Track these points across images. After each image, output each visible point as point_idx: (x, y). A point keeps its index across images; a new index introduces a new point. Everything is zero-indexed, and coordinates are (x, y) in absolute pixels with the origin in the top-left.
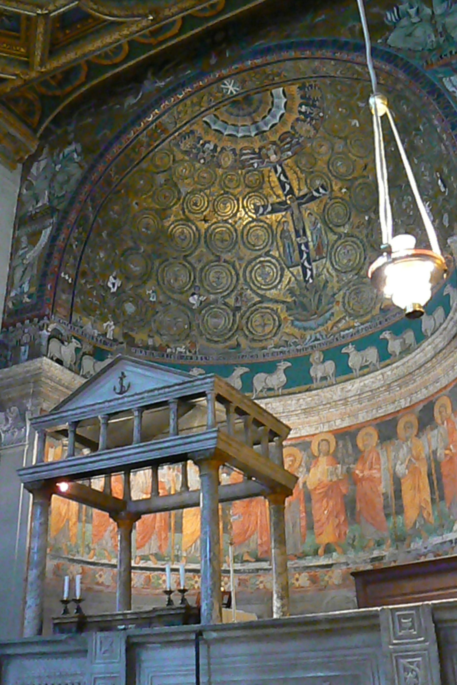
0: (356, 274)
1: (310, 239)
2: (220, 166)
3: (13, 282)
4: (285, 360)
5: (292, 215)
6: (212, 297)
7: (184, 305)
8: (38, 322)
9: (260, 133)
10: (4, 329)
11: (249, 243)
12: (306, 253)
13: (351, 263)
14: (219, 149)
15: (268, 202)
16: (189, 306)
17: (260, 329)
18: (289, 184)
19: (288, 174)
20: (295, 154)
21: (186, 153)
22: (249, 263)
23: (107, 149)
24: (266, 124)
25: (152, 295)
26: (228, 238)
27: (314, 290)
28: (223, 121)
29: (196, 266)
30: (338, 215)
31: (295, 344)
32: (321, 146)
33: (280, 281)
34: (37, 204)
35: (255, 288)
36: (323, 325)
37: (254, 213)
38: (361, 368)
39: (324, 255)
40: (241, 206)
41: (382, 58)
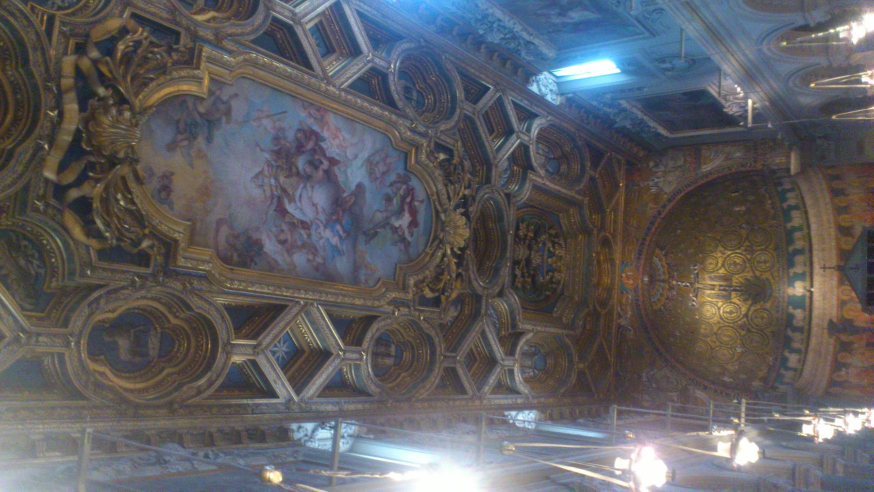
6: (739, 341)
9: (664, 281)
16: (742, 353)
17: (765, 320)
38: (805, 265)
41: (676, 196)
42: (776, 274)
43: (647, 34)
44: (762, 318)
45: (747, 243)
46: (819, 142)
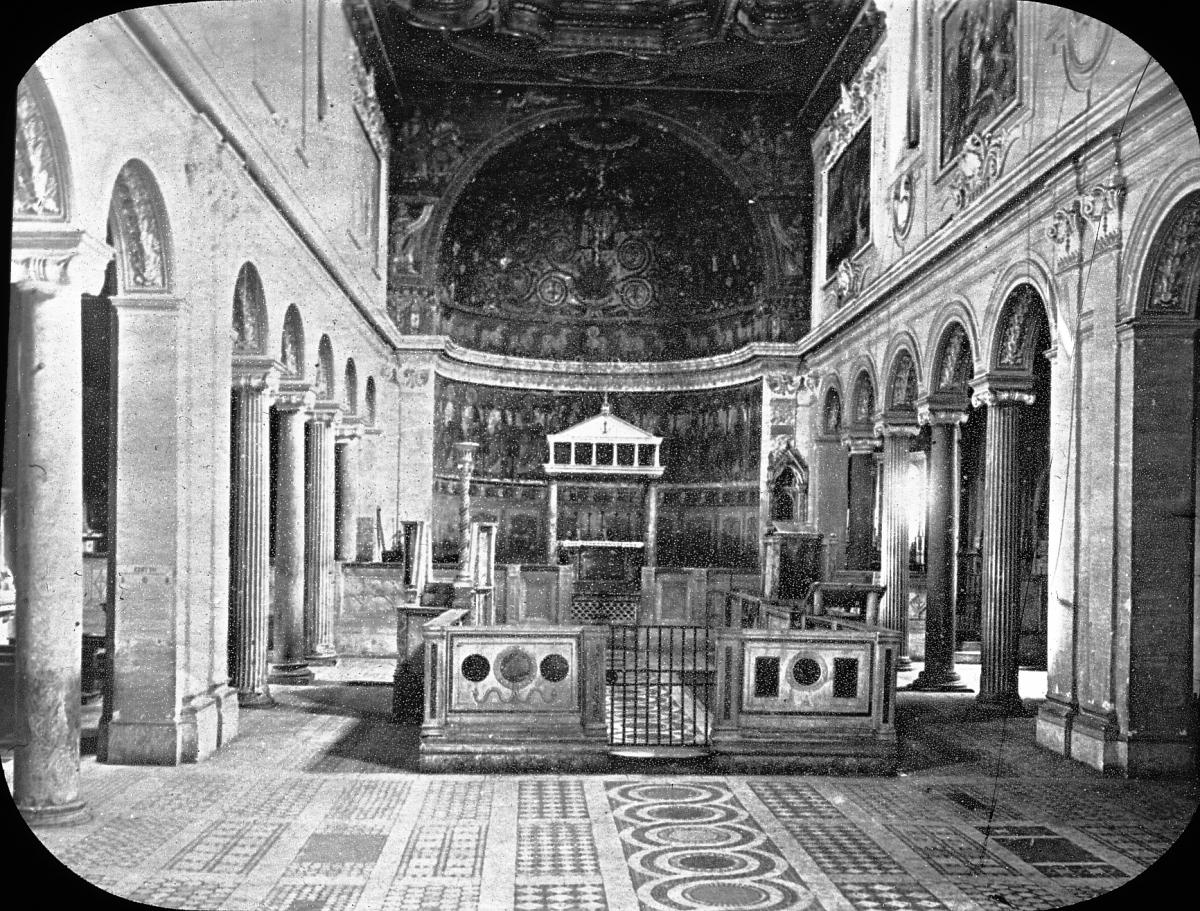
17: (550, 296)
43: (940, 173)
44: (554, 293)
46: (797, 379)
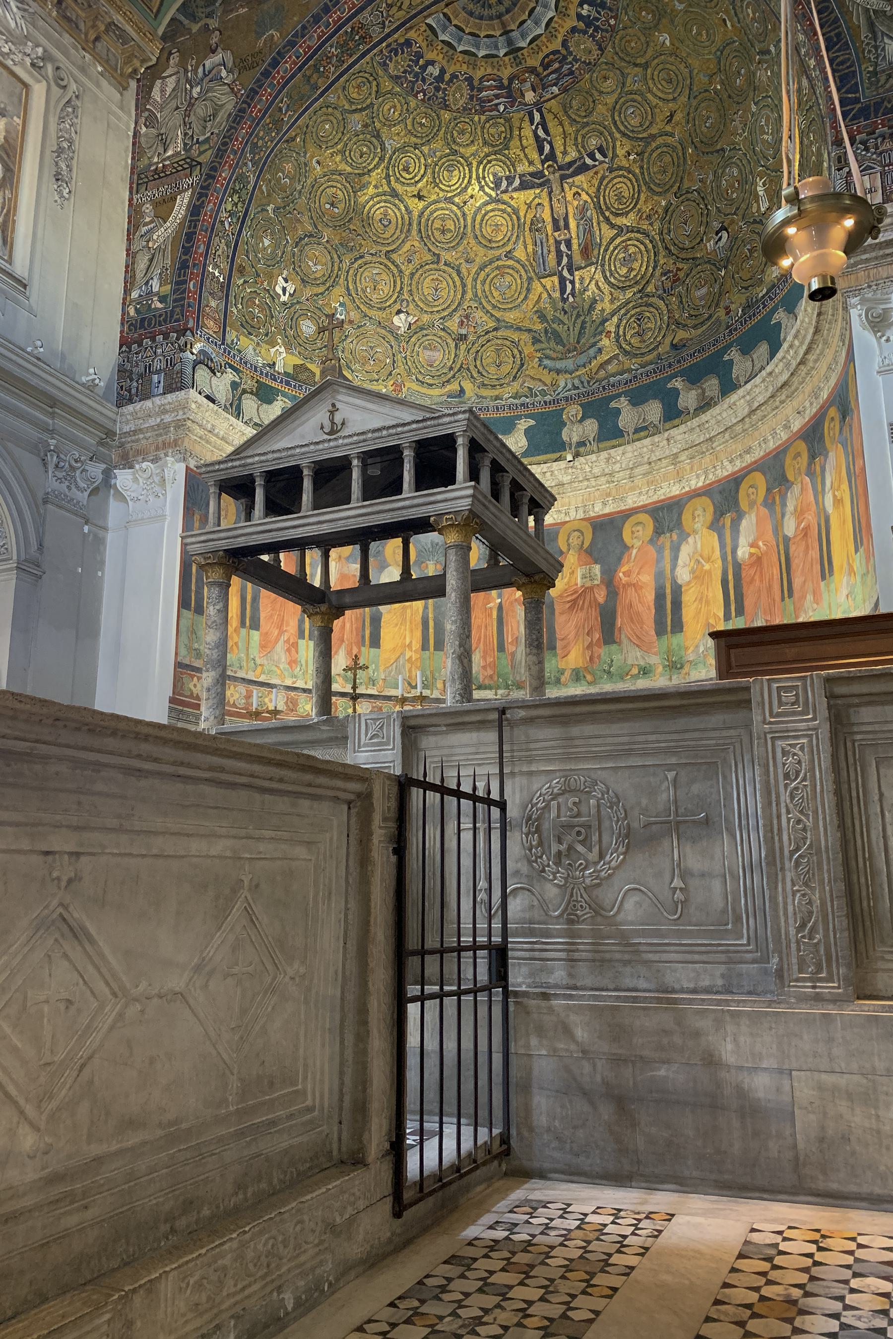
0: (640, 291)
1: (574, 235)
2: (446, 107)
3: (133, 277)
4: (526, 417)
5: (550, 193)
6: (426, 318)
7: (384, 328)
8: (178, 339)
9: (514, 51)
10: (124, 348)
11: (483, 236)
12: (567, 255)
13: (633, 273)
14: (447, 77)
15: (515, 170)
17: (492, 370)
18: (550, 143)
19: (550, 125)
20: (564, 90)
21: (396, 79)
22: (482, 269)
23: (275, 63)
24: (523, 36)
25: (340, 309)
26: (452, 228)
27: (575, 313)
28: (457, 27)
29: (403, 267)
30: (619, 197)
31: (543, 393)
32: (606, 78)
33: (526, 298)
34: (165, 151)
35: (489, 308)
36: (584, 366)
37: (492, 189)
38: (637, 431)
39: (594, 260)
40: (474, 176)
42: (611, 368)
45: (685, 266)
